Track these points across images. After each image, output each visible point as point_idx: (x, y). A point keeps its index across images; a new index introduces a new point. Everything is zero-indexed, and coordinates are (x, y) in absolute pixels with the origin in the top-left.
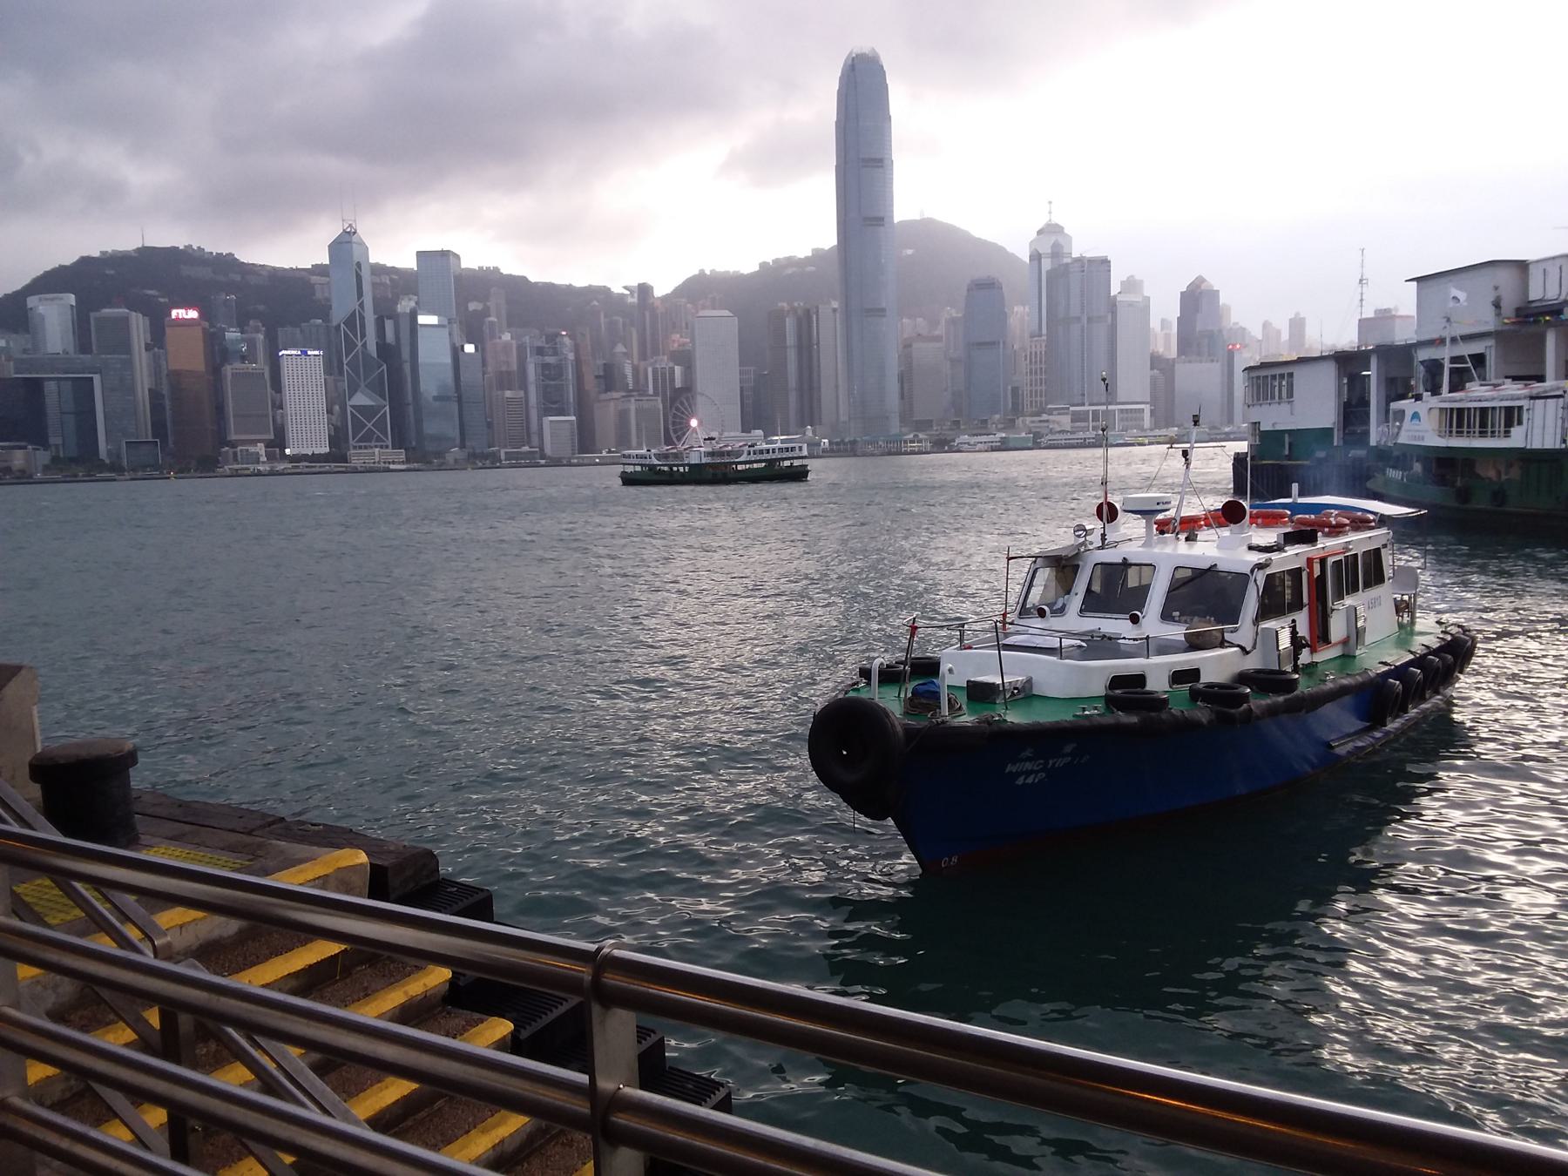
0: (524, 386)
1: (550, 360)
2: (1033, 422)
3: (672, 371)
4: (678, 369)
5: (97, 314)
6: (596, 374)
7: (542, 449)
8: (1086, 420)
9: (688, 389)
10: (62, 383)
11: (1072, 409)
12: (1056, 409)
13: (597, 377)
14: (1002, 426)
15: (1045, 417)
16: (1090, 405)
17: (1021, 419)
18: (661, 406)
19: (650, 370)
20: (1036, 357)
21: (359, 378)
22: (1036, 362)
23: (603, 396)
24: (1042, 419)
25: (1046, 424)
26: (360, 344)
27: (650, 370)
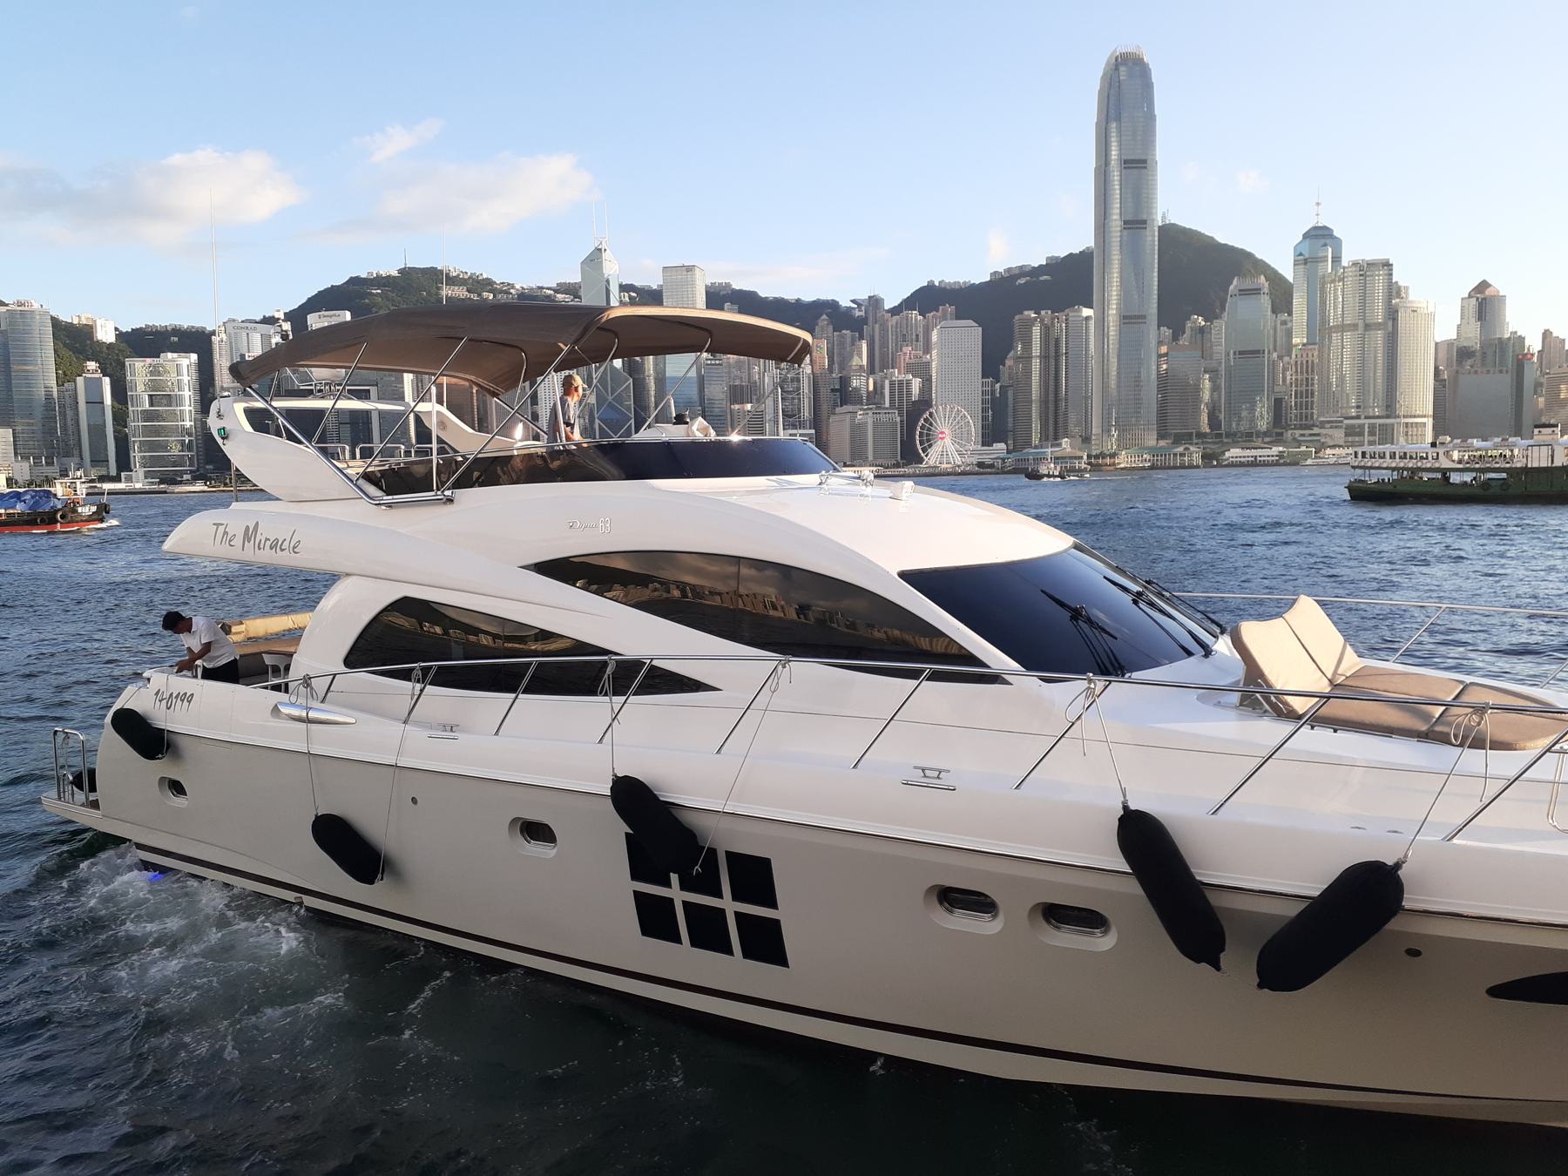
2: (1303, 435)
3: (909, 383)
4: (916, 384)
8: (1361, 434)
9: (925, 403)
11: (1346, 422)
12: (1329, 422)
13: (832, 390)
15: (1316, 430)
16: (1366, 418)
17: (1290, 432)
18: (898, 419)
19: (887, 382)
20: (1307, 367)
21: (607, 392)
23: (838, 410)
25: (1318, 438)
27: (887, 382)
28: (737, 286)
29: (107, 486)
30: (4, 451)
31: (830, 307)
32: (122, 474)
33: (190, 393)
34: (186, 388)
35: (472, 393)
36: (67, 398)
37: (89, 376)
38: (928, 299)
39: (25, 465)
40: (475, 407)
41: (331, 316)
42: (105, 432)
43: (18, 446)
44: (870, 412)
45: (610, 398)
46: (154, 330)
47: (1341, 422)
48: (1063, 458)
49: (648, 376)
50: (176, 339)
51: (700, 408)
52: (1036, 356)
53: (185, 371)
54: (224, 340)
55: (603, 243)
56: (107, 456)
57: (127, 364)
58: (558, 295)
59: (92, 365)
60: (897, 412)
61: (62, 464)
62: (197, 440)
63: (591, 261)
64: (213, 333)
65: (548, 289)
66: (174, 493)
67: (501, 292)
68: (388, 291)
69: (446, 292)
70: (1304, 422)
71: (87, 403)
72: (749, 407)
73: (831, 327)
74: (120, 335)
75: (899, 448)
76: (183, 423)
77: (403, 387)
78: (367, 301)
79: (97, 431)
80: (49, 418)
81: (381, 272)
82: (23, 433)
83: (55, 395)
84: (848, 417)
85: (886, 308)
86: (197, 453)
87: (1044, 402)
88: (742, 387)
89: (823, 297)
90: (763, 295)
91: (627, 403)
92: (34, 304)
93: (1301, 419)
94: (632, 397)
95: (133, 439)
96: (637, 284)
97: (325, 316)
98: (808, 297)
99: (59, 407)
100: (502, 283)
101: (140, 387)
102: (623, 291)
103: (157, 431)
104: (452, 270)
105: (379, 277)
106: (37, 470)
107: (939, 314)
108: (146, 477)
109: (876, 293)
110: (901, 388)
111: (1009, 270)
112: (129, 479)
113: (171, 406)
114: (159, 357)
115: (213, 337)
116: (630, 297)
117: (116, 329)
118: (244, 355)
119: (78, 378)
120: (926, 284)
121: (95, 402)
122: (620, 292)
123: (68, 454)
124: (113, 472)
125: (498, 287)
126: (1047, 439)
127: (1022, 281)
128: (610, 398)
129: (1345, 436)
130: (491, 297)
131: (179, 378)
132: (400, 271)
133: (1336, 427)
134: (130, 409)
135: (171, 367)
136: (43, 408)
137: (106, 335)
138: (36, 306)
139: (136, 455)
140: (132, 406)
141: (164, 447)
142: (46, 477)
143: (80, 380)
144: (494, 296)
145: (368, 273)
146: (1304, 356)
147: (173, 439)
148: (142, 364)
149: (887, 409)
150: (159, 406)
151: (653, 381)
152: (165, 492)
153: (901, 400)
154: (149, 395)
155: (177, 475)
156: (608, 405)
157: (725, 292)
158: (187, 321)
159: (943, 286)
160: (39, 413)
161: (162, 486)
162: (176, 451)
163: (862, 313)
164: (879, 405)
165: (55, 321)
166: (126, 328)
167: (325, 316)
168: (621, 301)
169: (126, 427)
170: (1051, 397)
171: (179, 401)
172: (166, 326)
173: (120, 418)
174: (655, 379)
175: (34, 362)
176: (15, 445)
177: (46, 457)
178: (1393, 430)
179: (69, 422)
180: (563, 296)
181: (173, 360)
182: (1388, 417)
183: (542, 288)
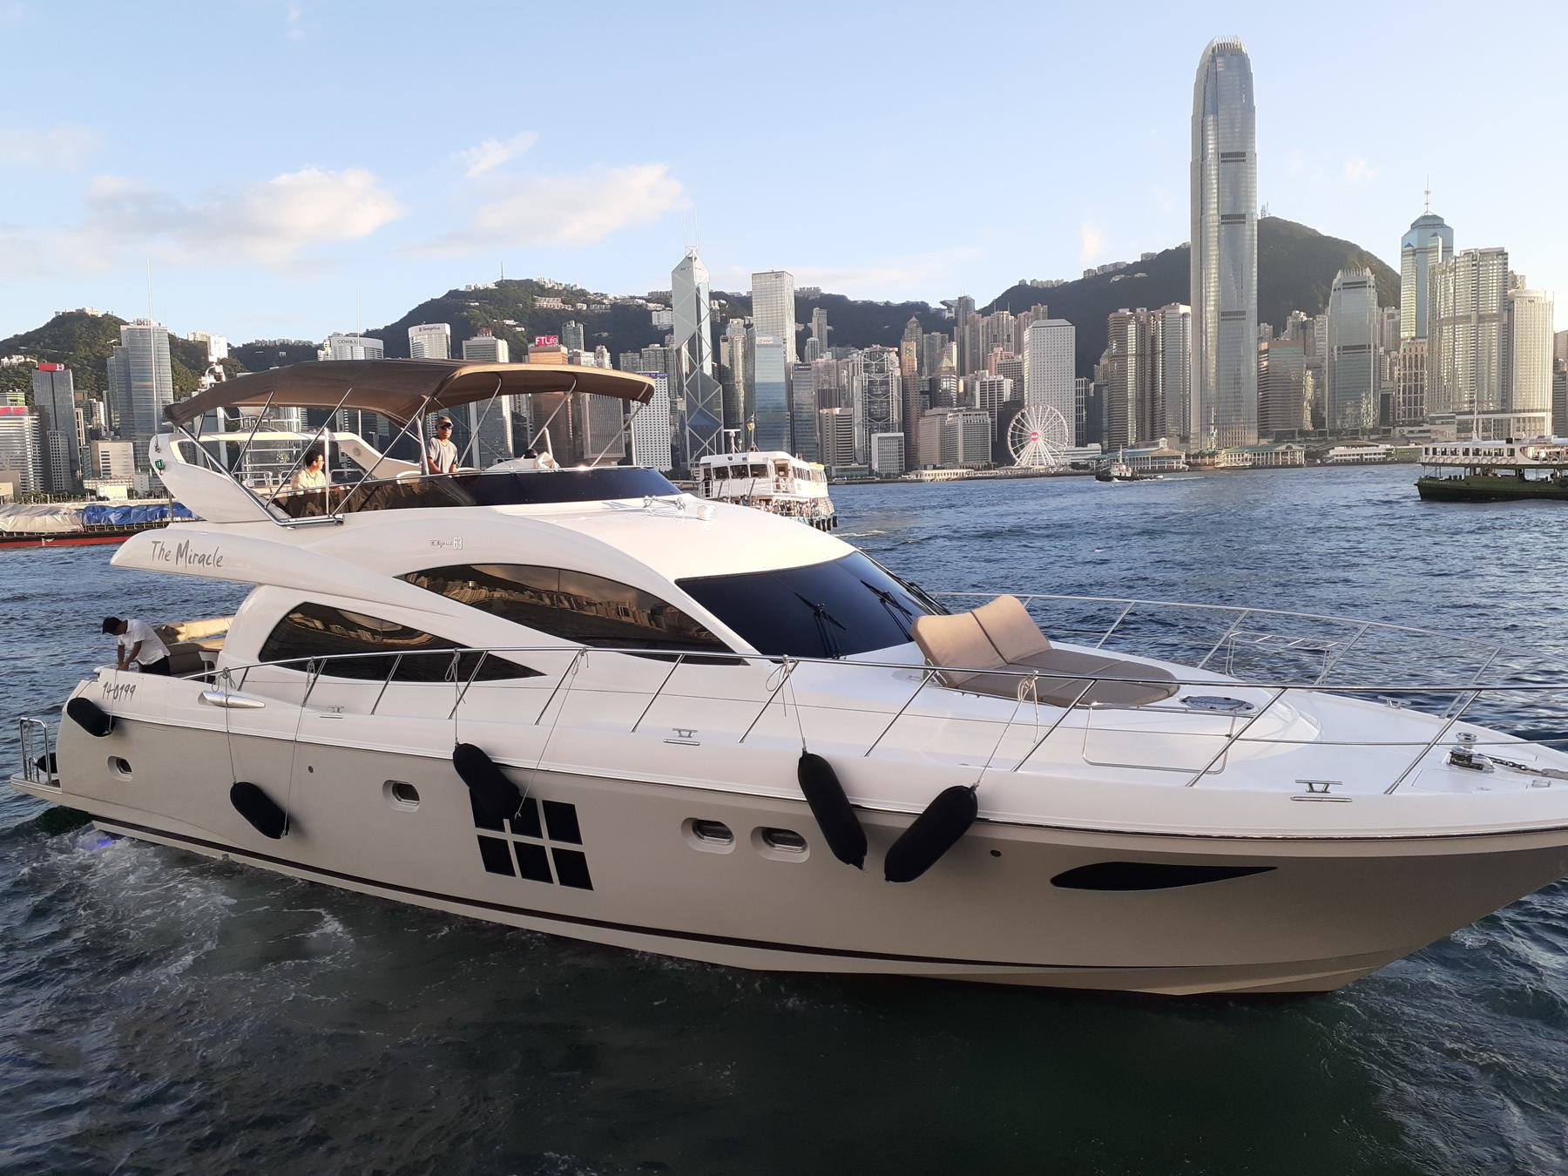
0: (849, 404)
1: (878, 378)
2: (1412, 432)
3: (1000, 384)
4: (1008, 385)
5: (468, 343)
6: (921, 389)
7: (870, 466)
9: (1017, 404)
11: (1458, 417)
13: (922, 393)
14: (1377, 437)
15: (1426, 427)
17: (1398, 429)
18: (989, 420)
19: (978, 384)
20: (1416, 361)
22: (1416, 366)
23: (928, 412)
24: (1421, 428)
25: (1428, 435)
26: (698, 366)
27: (978, 384)
28: (826, 290)
30: (126, 464)
31: (920, 310)
38: (1020, 299)
39: (145, 477)
41: (431, 329)
44: (960, 414)
45: (700, 405)
47: (1454, 417)
48: (1159, 458)
50: (284, 353)
52: (1133, 355)
60: (987, 413)
64: (321, 347)
65: (640, 298)
67: (595, 302)
68: (486, 303)
69: (545, 303)
70: (1413, 419)
72: (837, 411)
73: (920, 330)
74: (233, 351)
75: (990, 450)
78: (465, 313)
84: (938, 419)
85: (977, 309)
87: (1140, 401)
88: (831, 390)
89: (913, 299)
90: (851, 298)
93: (1410, 416)
96: (728, 291)
97: (425, 329)
98: (897, 300)
102: (713, 299)
104: (547, 282)
105: (477, 290)
107: (1031, 314)
109: (966, 294)
110: (992, 389)
111: (1103, 267)
116: (720, 305)
117: (229, 345)
120: (1017, 284)
122: (710, 300)
125: (592, 297)
126: (1143, 439)
127: (1116, 279)
128: (700, 405)
129: (1458, 432)
130: (585, 307)
132: (497, 284)
133: (1448, 423)
138: (154, 324)
144: (588, 307)
146: (1414, 349)
149: (977, 410)
151: (742, 388)
153: (992, 401)
157: (813, 297)
159: (1035, 285)
163: (953, 315)
164: (970, 406)
165: (172, 340)
166: (237, 344)
167: (425, 329)
168: (711, 309)
170: (1148, 397)
172: (275, 342)
178: (1509, 425)
180: (655, 305)
182: (1503, 411)
183: (636, 298)
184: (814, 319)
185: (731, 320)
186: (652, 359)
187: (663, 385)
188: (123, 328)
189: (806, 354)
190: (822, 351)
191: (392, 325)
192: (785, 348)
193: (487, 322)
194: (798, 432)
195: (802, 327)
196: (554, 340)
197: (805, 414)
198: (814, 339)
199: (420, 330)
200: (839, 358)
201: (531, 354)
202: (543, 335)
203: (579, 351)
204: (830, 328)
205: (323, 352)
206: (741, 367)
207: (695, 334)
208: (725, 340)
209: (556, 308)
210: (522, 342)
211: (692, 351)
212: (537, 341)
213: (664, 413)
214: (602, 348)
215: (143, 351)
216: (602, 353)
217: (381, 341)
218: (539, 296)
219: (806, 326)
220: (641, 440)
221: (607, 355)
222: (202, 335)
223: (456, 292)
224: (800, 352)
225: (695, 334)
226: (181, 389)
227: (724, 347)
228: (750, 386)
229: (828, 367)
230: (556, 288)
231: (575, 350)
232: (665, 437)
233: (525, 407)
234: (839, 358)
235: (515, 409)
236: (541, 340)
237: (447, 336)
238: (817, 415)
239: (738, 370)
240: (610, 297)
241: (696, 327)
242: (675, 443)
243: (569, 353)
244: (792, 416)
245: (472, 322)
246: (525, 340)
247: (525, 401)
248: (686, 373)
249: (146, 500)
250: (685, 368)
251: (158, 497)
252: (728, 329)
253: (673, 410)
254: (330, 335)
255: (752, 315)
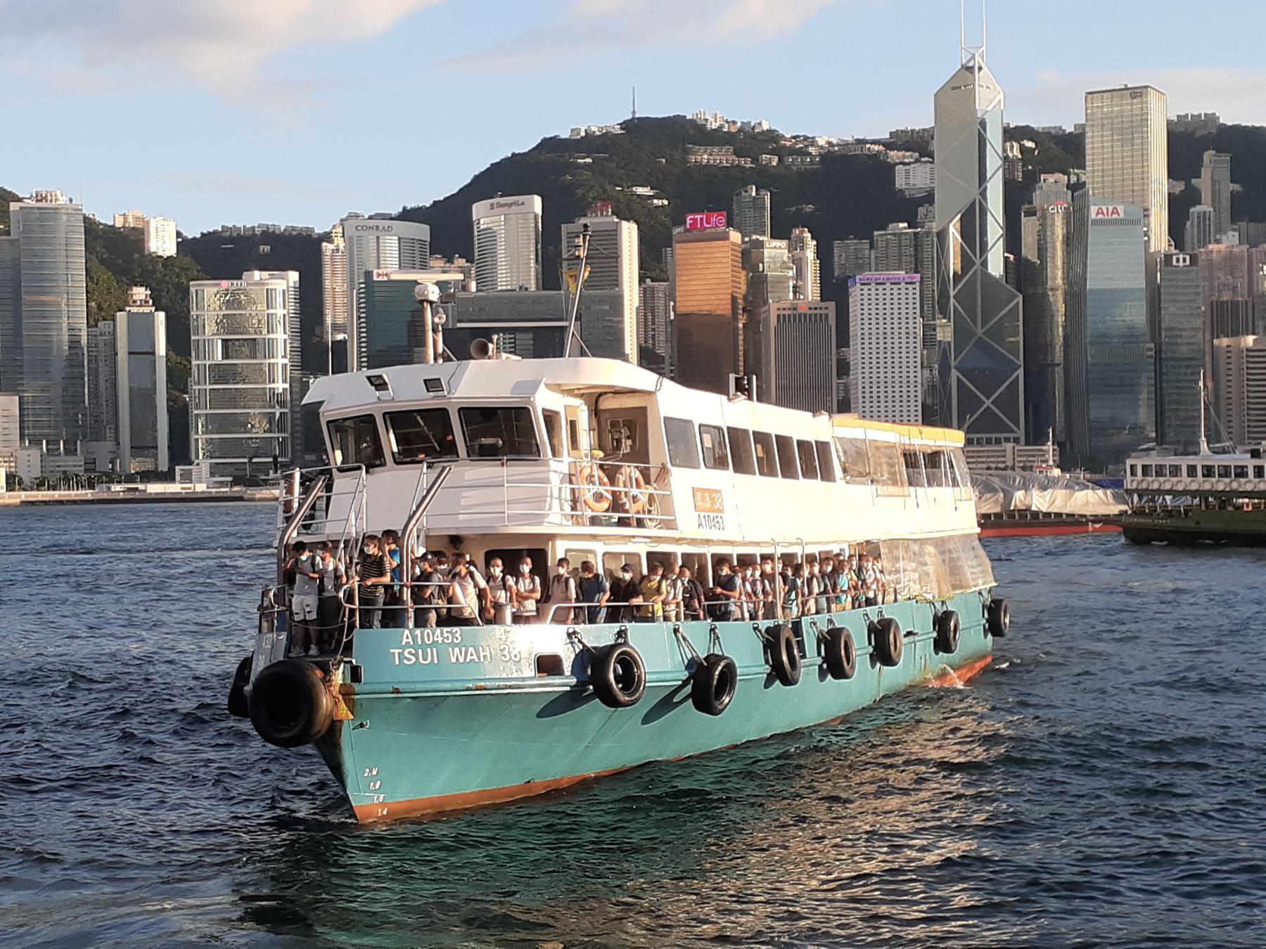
10: (519, 336)
26: (978, 261)
28: (1227, 119)
29: (154, 488)
32: (177, 468)
33: (286, 337)
34: (280, 328)
35: (736, 328)
36: (101, 345)
37: (134, 310)
40: (741, 353)
42: (154, 400)
43: (26, 424)
45: (980, 332)
46: (235, 234)
49: (1052, 290)
50: (267, 248)
51: (1152, 345)
53: (280, 300)
54: (341, 248)
55: (977, 56)
56: (155, 438)
57: (193, 290)
58: (892, 153)
59: (140, 293)
61: (88, 452)
62: (293, 412)
63: (954, 88)
64: (327, 237)
65: (874, 142)
66: (253, 500)
67: (792, 151)
68: (605, 159)
71: (130, 353)
72: (1250, 340)
76: (272, 386)
77: (622, 322)
79: (142, 398)
80: (74, 379)
81: (594, 129)
82: (33, 402)
83: (84, 340)
86: (292, 434)
88: (1235, 305)
91: (1012, 339)
92: (59, 197)
94: (1021, 328)
95: (196, 412)
99: (89, 361)
100: (794, 137)
101: (210, 328)
102: (1010, 139)
103: (233, 399)
106: (51, 463)
108: (212, 474)
112: (187, 477)
113: (255, 357)
114: (240, 278)
115: (324, 244)
116: (1023, 150)
117: (179, 234)
118: (372, 272)
119: (118, 314)
121: (143, 352)
122: (1005, 141)
123: (98, 437)
124: (163, 466)
125: (788, 144)
128: (980, 332)
131: (271, 311)
132: (626, 125)
134: (194, 363)
135: (259, 294)
136: (64, 363)
137: (162, 244)
138: (62, 200)
139: (200, 437)
140: (198, 358)
141: (240, 423)
142: (64, 472)
143: (121, 316)
144: (779, 160)
145: (572, 130)
147: (257, 411)
148: (216, 290)
150: (237, 358)
151: (1061, 299)
152: (241, 499)
154: (223, 340)
155: (259, 471)
156: (976, 344)
157: (1205, 132)
158: (284, 218)
160: (58, 369)
161: (236, 489)
162: (259, 431)
165: (90, 226)
166: (192, 233)
169: (187, 393)
171: (268, 349)
172: (253, 228)
173: (179, 377)
174: (1066, 293)
175: (54, 290)
176: (21, 422)
177: (64, 442)
179: (102, 385)
180: (901, 153)
181: (261, 283)
183: (864, 142)
184: (1206, 172)
185: (1042, 177)
186: (893, 251)
187: (910, 296)
188: (14, 206)
189: (1188, 237)
190: (1219, 230)
191: (446, 199)
192: (1148, 226)
193: (605, 191)
194: (1168, 381)
195: (1180, 187)
196: (718, 219)
197: (1184, 349)
198: (1205, 207)
199: (492, 207)
200: (1253, 245)
201: (677, 246)
202: (701, 212)
203: (761, 238)
204: (1237, 187)
205: (331, 246)
206: (1059, 263)
207: (973, 204)
208: (1031, 213)
209: (725, 164)
210: (663, 224)
211: (966, 232)
212: (688, 222)
213: (911, 346)
214: (802, 232)
215: (44, 244)
216: (802, 240)
217: (428, 227)
218: (694, 144)
219: (1189, 186)
220: (867, 395)
221: (812, 244)
222: (136, 219)
223: (554, 140)
224: (1176, 231)
225: (973, 204)
226: (100, 308)
227: (1029, 227)
228: (1076, 294)
229: (1230, 259)
230: (725, 130)
231: (754, 237)
232: (912, 389)
233: (662, 338)
234: (1253, 245)
235: (646, 342)
236: (695, 220)
237: (536, 216)
238: (1208, 348)
239: (1055, 267)
240: (821, 142)
241: (977, 191)
242: (929, 401)
243: (743, 242)
244: (1158, 351)
245: (580, 192)
246: (668, 221)
247: (662, 328)
248: (955, 273)
249: (35, 493)
250: (954, 264)
251: (54, 489)
252: (1038, 192)
253: (928, 340)
254: (343, 217)
255: (1083, 167)
